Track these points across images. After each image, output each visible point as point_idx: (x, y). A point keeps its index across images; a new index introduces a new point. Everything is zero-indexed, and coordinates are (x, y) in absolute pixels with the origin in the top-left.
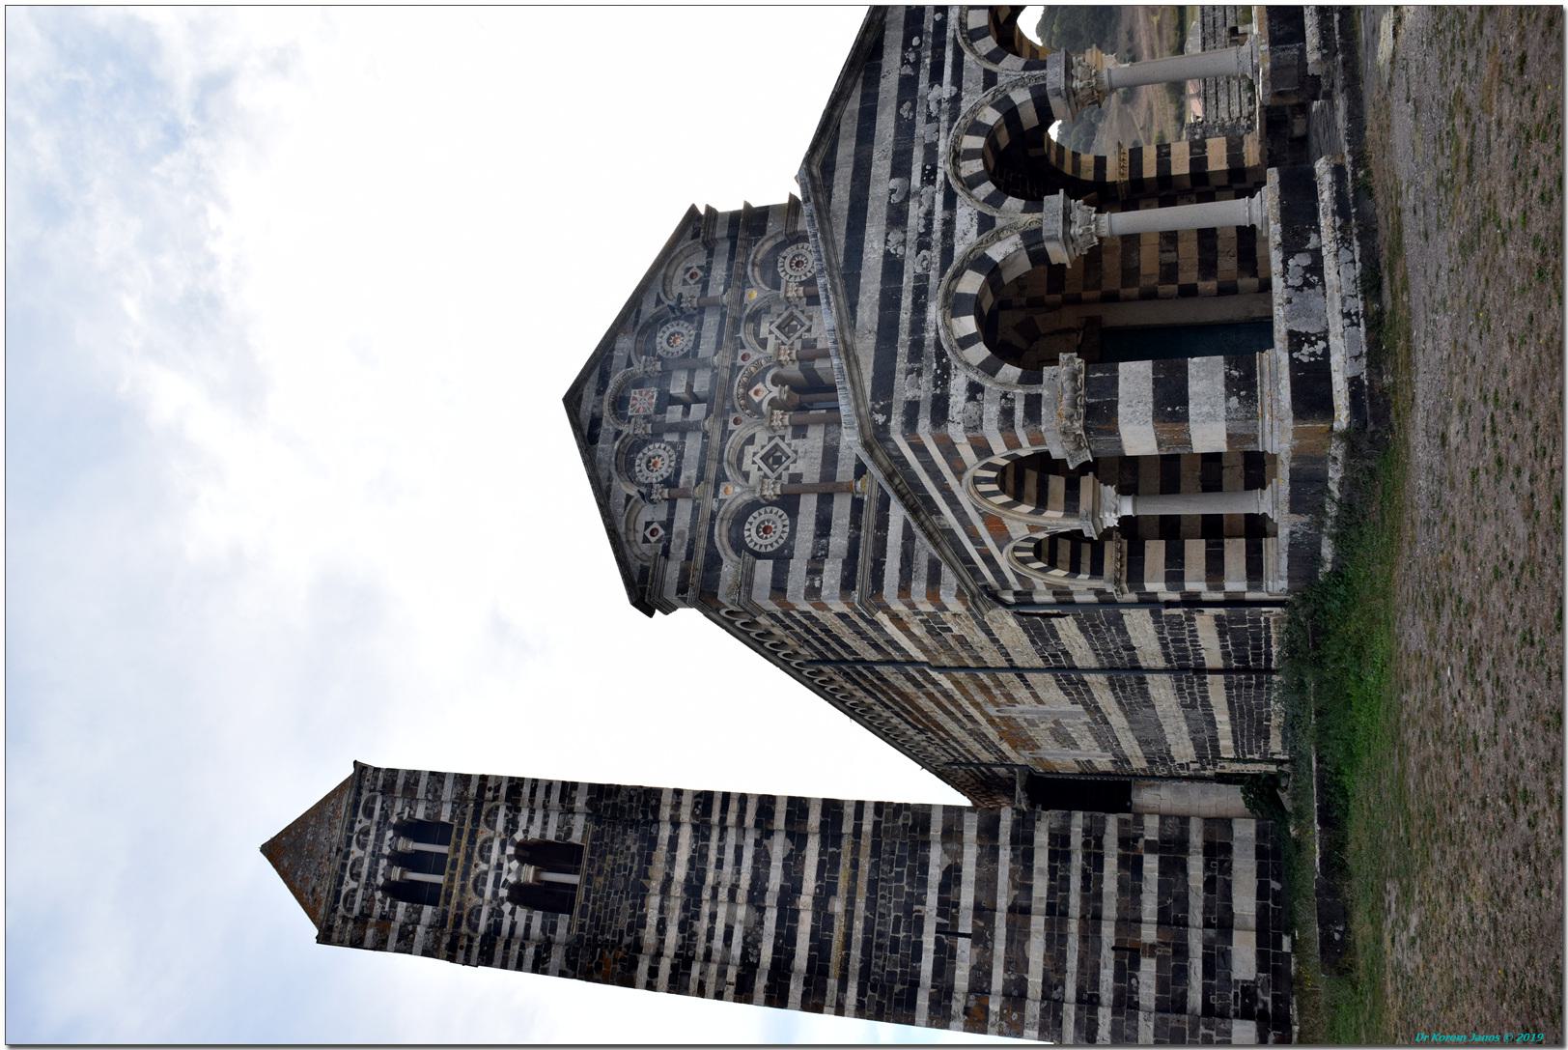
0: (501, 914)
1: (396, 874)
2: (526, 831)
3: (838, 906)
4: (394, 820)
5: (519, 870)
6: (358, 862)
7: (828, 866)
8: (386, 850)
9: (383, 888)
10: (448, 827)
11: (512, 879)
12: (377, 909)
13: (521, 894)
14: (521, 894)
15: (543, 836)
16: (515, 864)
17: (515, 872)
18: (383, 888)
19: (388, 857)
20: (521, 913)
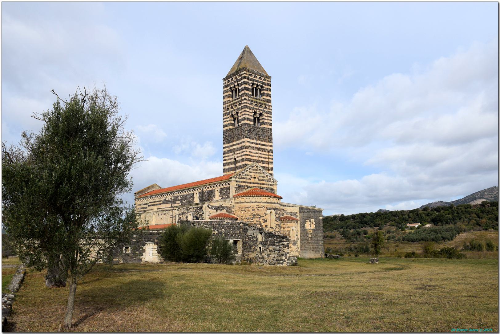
6: (256, 77)
12: (250, 82)
17: (258, 112)
20: (252, 114)
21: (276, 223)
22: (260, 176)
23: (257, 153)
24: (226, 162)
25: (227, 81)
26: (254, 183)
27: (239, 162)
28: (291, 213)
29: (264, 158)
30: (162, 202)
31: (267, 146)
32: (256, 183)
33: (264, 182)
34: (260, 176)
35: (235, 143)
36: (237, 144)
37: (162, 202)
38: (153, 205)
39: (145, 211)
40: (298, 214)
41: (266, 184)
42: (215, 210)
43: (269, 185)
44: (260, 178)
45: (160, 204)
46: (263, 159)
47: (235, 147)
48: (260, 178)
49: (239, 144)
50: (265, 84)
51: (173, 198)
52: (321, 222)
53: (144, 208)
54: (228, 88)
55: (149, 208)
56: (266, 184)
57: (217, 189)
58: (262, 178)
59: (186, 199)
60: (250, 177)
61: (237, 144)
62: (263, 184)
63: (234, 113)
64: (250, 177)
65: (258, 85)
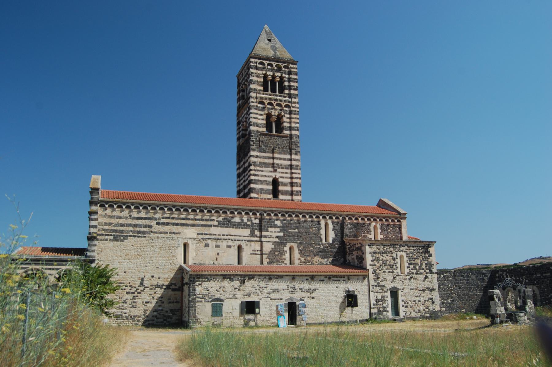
24: (256, 178)
25: (259, 61)
27: (285, 185)
30: (216, 223)
35: (276, 155)
36: (281, 159)
37: (216, 223)
38: (177, 224)
39: (139, 232)
45: (210, 226)
47: (276, 161)
49: (284, 159)
51: (257, 221)
53: (135, 226)
54: (259, 72)
55: (156, 228)
57: (373, 224)
59: (297, 227)
61: (281, 159)
63: (275, 113)
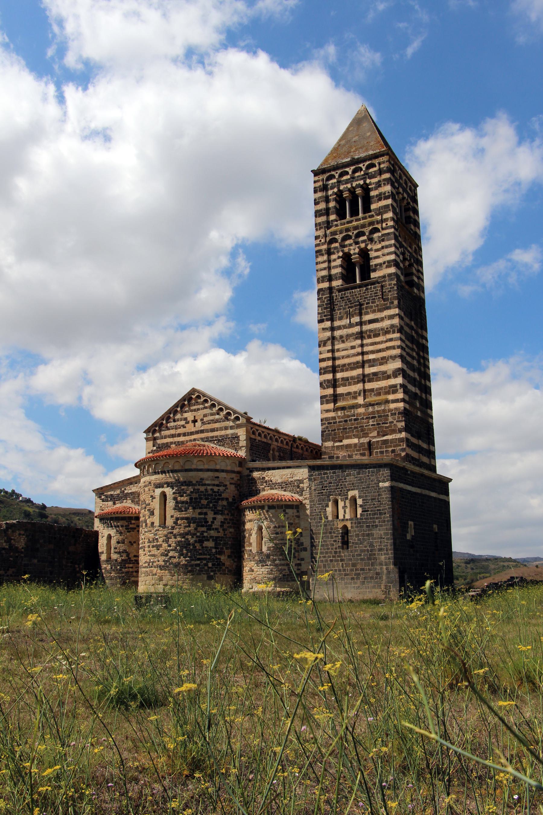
0: (338, 252)
1: (346, 194)
2: (371, 250)
3: (360, 400)
4: (368, 181)
5: (355, 254)
6: (347, 173)
7: (378, 392)
8: (354, 184)
9: (339, 190)
10: (370, 211)
11: (352, 252)
13: (347, 257)
14: (347, 257)
15: (372, 259)
16: (357, 250)
17: (354, 250)
18: (339, 190)
19: (352, 187)
20: (339, 262)
21: (178, 514)
22: (205, 416)
23: (353, 347)
26: (192, 433)
28: (284, 485)
29: (373, 352)
31: (382, 319)
32: (197, 432)
33: (217, 425)
34: (205, 416)
40: (305, 485)
41: (221, 429)
42: (110, 503)
43: (226, 428)
44: (205, 419)
46: (371, 357)
48: (205, 419)
50: (372, 177)
52: (386, 497)
56: (221, 429)
58: (211, 418)
60: (183, 423)
62: (213, 430)
64: (183, 423)
65: (352, 191)
